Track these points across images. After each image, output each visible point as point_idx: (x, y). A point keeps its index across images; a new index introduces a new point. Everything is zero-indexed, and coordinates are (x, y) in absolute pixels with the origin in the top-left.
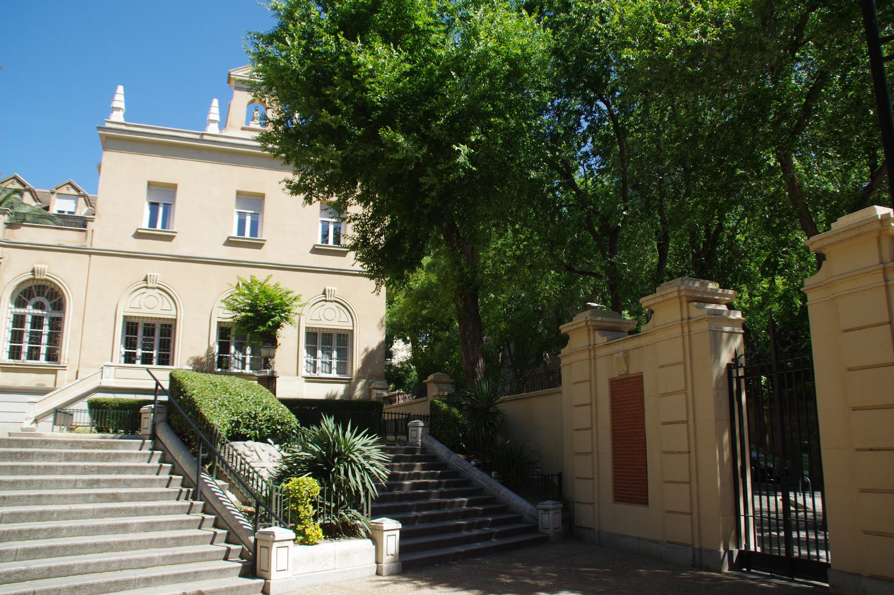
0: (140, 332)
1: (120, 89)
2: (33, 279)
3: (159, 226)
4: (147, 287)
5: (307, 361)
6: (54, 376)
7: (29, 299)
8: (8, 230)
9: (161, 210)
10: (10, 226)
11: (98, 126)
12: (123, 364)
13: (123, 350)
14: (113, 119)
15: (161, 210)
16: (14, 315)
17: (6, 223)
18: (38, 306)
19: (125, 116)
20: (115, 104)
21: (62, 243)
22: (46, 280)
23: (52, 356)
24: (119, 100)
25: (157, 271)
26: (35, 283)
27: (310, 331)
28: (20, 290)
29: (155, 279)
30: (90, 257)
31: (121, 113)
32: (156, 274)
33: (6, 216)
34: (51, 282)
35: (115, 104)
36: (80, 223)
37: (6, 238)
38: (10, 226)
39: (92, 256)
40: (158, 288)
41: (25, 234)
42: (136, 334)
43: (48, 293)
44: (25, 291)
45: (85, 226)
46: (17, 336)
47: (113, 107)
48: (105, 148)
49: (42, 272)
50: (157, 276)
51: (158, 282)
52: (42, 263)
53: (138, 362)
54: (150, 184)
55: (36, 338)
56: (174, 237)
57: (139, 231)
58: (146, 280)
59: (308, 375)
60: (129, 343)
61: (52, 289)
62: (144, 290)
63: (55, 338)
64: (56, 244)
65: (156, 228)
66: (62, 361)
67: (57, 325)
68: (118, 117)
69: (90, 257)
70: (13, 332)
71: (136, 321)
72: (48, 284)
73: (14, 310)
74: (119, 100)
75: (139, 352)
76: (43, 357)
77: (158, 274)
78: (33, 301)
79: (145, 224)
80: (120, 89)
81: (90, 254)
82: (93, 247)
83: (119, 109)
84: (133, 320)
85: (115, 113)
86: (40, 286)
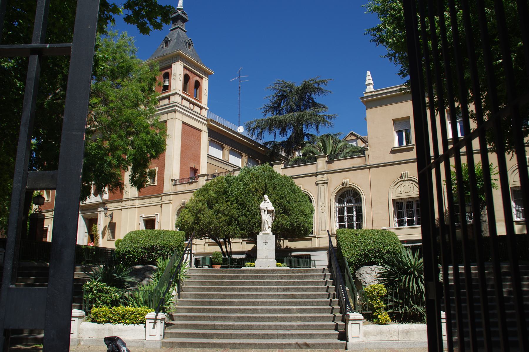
0: (405, 207)
1: (368, 73)
2: (344, 188)
3: (405, 144)
4: (403, 181)
5: (516, 210)
9: (404, 133)
10: (328, 162)
12: (397, 227)
13: (397, 219)
14: (367, 91)
15: (404, 133)
17: (326, 162)
19: (374, 87)
20: (367, 82)
24: (369, 79)
27: (515, 189)
28: (339, 195)
29: (406, 175)
30: (369, 170)
31: (371, 86)
34: (353, 188)
35: (367, 82)
36: (362, 152)
37: (328, 169)
38: (328, 162)
40: (409, 180)
41: (337, 165)
45: (364, 153)
46: (341, 219)
47: (366, 84)
49: (347, 183)
50: (407, 173)
51: (408, 176)
52: (346, 178)
53: (406, 225)
54: (394, 121)
55: (350, 219)
57: (393, 149)
58: (401, 176)
59: (519, 219)
60: (399, 214)
61: (354, 191)
62: (402, 182)
63: (360, 218)
64: (351, 167)
67: (359, 210)
68: (370, 88)
69: (369, 170)
70: (339, 217)
72: (351, 189)
73: (337, 206)
74: (369, 79)
75: (406, 219)
78: (346, 200)
79: (396, 144)
80: (368, 73)
81: (369, 168)
82: (370, 164)
83: (369, 84)
84: (400, 201)
85: (368, 87)
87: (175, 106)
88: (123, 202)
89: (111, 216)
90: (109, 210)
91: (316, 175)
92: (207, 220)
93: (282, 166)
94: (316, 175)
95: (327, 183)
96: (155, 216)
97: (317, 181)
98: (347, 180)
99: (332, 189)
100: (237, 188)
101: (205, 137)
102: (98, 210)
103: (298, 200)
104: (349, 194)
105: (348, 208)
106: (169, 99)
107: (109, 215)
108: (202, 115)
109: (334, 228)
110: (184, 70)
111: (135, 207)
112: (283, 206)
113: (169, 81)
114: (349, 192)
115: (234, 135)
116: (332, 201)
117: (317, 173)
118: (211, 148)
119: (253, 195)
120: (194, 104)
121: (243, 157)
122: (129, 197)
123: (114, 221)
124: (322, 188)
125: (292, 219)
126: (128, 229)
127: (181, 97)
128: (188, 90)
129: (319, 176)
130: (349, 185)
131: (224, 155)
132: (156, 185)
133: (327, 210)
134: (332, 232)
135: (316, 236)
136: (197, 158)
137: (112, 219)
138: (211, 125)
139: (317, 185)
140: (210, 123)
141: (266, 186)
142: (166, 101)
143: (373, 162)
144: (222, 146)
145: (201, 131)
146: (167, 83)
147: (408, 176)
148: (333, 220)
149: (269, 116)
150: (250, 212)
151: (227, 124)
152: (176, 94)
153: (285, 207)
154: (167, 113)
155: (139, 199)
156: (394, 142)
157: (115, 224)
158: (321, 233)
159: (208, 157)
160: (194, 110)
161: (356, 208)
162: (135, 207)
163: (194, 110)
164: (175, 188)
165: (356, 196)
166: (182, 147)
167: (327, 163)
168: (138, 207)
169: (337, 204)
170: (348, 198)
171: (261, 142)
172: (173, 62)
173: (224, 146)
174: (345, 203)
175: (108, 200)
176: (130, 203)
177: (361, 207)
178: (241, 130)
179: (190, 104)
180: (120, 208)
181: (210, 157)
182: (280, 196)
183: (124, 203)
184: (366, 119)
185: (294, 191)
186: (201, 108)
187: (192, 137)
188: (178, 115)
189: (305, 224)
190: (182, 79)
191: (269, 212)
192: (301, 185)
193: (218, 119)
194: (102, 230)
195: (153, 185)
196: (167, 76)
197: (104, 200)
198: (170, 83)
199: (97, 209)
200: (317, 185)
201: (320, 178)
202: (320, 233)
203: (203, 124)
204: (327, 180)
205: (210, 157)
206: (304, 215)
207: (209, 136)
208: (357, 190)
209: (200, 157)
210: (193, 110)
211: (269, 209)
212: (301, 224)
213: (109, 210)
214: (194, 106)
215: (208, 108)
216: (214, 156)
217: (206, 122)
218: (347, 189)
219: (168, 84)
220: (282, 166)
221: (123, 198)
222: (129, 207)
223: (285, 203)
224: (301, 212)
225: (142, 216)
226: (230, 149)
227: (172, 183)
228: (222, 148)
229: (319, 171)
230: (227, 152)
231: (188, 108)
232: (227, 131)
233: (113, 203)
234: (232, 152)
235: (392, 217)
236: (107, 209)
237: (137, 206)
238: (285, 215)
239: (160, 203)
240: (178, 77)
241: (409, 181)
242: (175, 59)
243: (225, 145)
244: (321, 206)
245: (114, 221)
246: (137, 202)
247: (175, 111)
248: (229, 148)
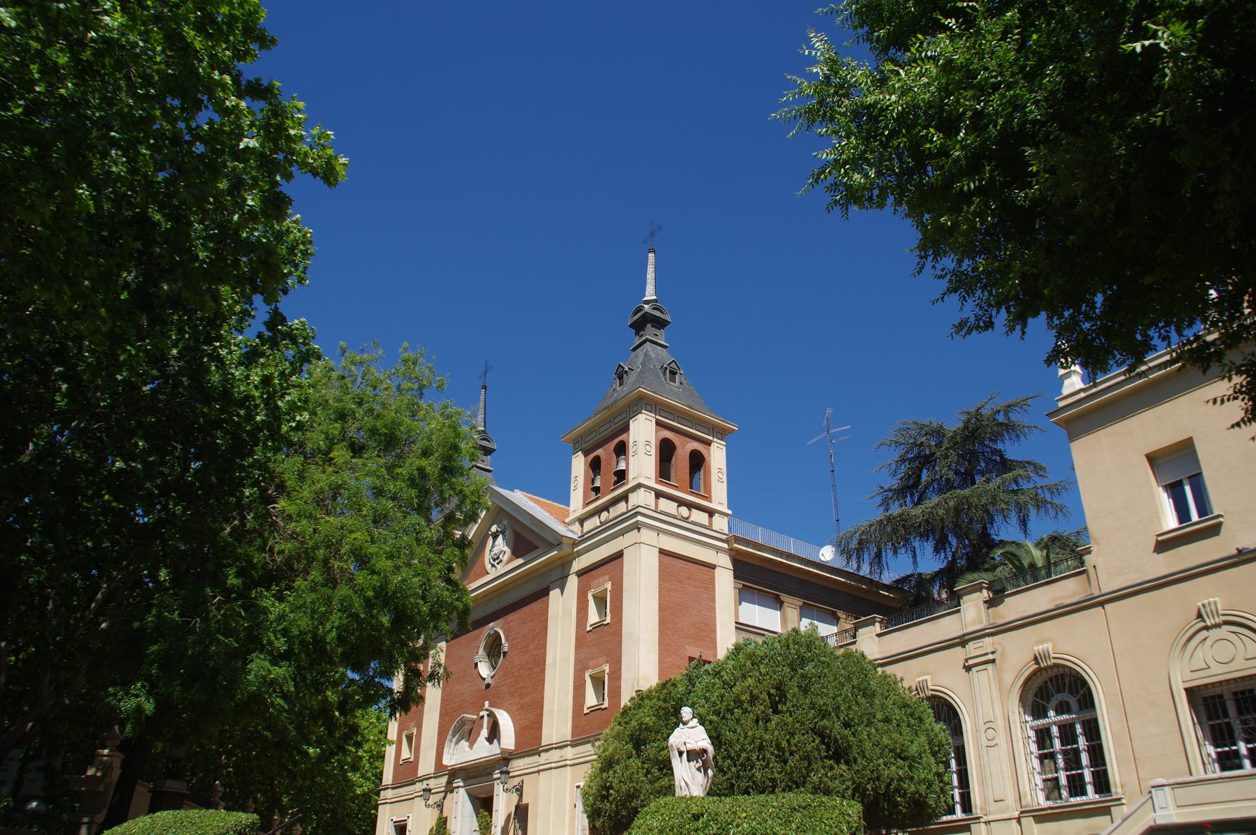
3: (1195, 517)
6: (1109, 817)
7: (1048, 700)
8: (990, 610)
9: (1188, 489)
10: (991, 603)
11: (1046, 413)
14: (1065, 392)
15: (1188, 489)
16: (1036, 731)
17: (985, 602)
18: (1062, 708)
21: (1059, 602)
22: (1056, 665)
23: (1102, 784)
25: (1211, 593)
26: (1045, 676)
30: (1104, 608)
32: (1212, 600)
33: (985, 591)
34: (1064, 666)
37: (992, 622)
38: (991, 603)
39: (1106, 606)
41: (1017, 606)
42: (1226, 715)
43: (1070, 682)
44: (1040, 688)
45: (1082, 564)
47: (1061, 376)
48: (1073, 437)
49: (1046, 656)
50: (1215, 602)
51: (1221, 612)
54: (1152, 459)
55: (1073, 760)
56: (1219, 525)
57: (1160, 538)
58: (1200, 616)
62: (1204, 634)
64: (1052, 606)
65: (1191, 520)
66: (1113, 789)
67: (1092, 730)
69: (1104, 608)
70: (1042, 758)
71: (1218, 691)
72: (1061, 670)
76: (1090, 789)
77: (1217, 599)
78: (1054, 702)
79: (1170, 521)
81: (1102, 604)
82: (1104, 591)
84: (1211, 692)
85: (1067, 382)
86: (1056, 676)
87: (638, 513)
88: (542, 754)
89: (517, 790)
90: (511, 774)
91: (962, 641)
92: (624, 788)
93: (877, 628)
94: (962, 641)
95: (993, 661)
97: (966, 660)
98: (1045, 646)
99: (1008, 678)
100: (706, 698)
101: (725, 581)
102: (495, 776)
103: (879, 716)
104: (1058, 685)
105: (1059, 727)
106: (627, 502)
107: (515, 787)
108: (714, 528)
109: (1028, 789)
110: (656, 432)
111: (566, 766)
112: (829, 737)
113: (625, 459)
114: (1057, 680)
115: (807, 568)
116: (1013, 712)
117: (964, 635)
118: (745, 606)
119: (745, 711)
120: (690, 506)
121: (842, 621)
122: (554, 742)
123: (524, 801)
124: (982, 677)
125: (857, 772)
126: (551, 818)
127: (653, 493)
128: (673, 475)
129: (970, 644)
130: (1054, 661)
131: (784, 620)
132: (606, 708)
133: (1002, 739)
134: (1023, 803)
135: (979, 818)
136: (707, 632)
137: (521, 796)
138: (738, 551)
139: (968, 669)
140: (735, 545)
141: (779, 687)
142: (621, 507)
143: (1108, 582)
144: (777, 598)
145: (714, 569)
146: (622, 466)
147: (1221, 612)
148: (1021, 766)
149: (895, 510)
150: (732, 758)
151: (790, 544)
152: (639, 486)
153: (836, 740)
154: (622, 533)
155: (574, 744)
156: (1159, 518)
157: (526, 807)
158: (993, 807)
159: (736, 628)
160: (692, 519)
161: (1084, 724)
162: (566, 766)
163: (692, 519)
165: (1077, 692)
166: (662, 609)
167: (986, 605)
168: (571, 766)
169: (1029, 718)
170: (1057, 698)
171: (888, 578)
172: (632, 415)
173: (781, 597)
174: (1051, 713)
175: (515, 750)
176: (554, 755)
177: (1096, 720)
178: (827, 554)
179: (678, 506)
180: (536, 769)
181: (740, 627)
182: (820, 710)
183: (544, 757)
184: (1073, 469)
185: (869, 695)
186: (711, 513)
187: (689, 584)
188: (645, 535)
189: (906, 786)
190: (653, 451)
191: (693, 755)
192: (928, 674)
193: (760, 535)
194: (503, 824)
195: (600, 709)
196: (621, 450)
197: (504, 751)
198: (627, 465)
199: (491, 774)
200: (968, 669)
201: (973, 648)
202: (992, 809)
203: (718, 549)
204: (993, 653)
205: (740, 627)
206: (904, 759)
207: (735, 578)
208: (1078, 672)
209: (715, 631)
210: (690, 521)
211: (690, 747)
212: (889, 785)
213: (511, 774)
214: (690, 510)
215: (730, 512)
216: (757, 625)
217: (726, 546)
218: (1050, 672)
219: (624, 468)
220: (877, 628)
222: (553, 765)
223: (837, 729)
224: (891, 751)
225: (578, 787)
226: (801, 604)
228: (778, 604)
229: (970, 630)
230: (792, 613)
231: (675, 517)
232: (785, 561)
233: (524, 757)
234: (805, 611)
235: (1191, 743)
236: (508, 773)
237: (568, 762)
238: (838, 763)
240: (641, 448)
241: (1225, 628)
242: (635, 408)
243: (784, 597)
244: (983, 728)
245: (524, 801)
246: (569, 752)
247: (637, 527)
248: (799, 602)
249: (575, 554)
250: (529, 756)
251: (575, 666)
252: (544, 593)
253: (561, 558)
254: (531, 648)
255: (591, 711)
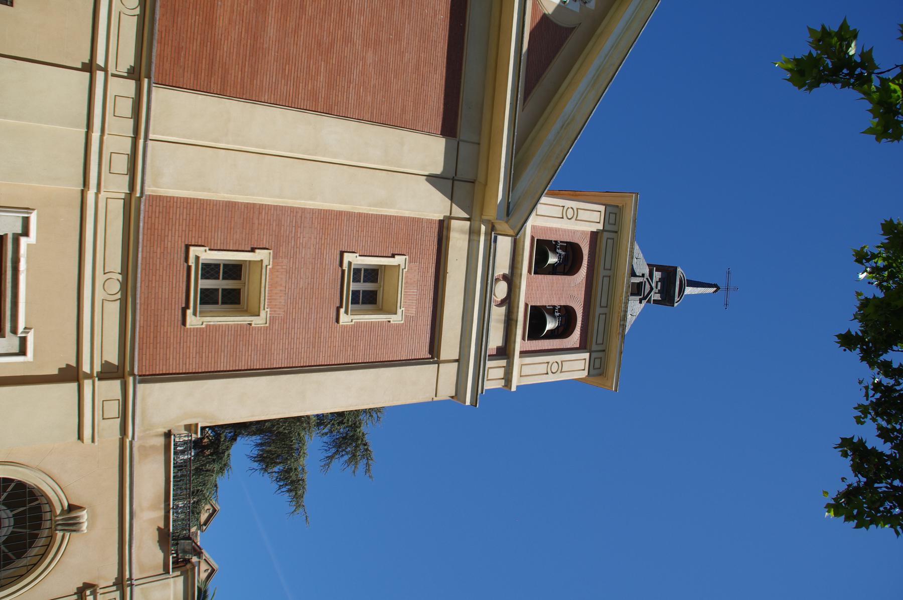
96: (14, 331)
132: (184, 323)
164: (153, 447)
180: (100, 61)
221: (154, 90)
222: (95, 135)
227: (181, 426)
239: (86, 368)
249: (476, 224)
250: (141, 19)
251: (292, 209)
252: (449, 130)
253: (486, 184)
254: (370, 56)
255: (189, 268)
